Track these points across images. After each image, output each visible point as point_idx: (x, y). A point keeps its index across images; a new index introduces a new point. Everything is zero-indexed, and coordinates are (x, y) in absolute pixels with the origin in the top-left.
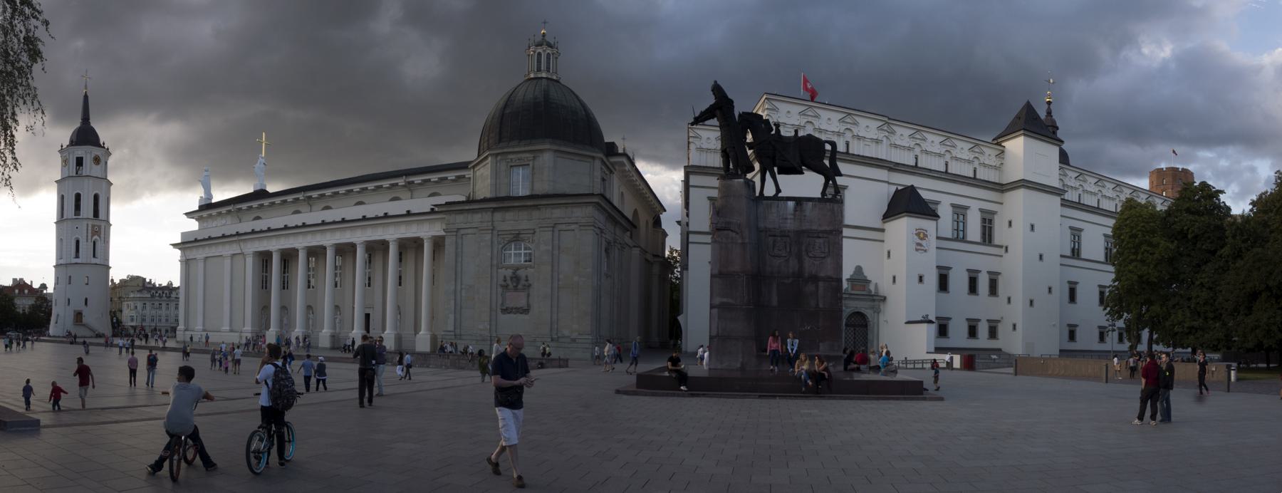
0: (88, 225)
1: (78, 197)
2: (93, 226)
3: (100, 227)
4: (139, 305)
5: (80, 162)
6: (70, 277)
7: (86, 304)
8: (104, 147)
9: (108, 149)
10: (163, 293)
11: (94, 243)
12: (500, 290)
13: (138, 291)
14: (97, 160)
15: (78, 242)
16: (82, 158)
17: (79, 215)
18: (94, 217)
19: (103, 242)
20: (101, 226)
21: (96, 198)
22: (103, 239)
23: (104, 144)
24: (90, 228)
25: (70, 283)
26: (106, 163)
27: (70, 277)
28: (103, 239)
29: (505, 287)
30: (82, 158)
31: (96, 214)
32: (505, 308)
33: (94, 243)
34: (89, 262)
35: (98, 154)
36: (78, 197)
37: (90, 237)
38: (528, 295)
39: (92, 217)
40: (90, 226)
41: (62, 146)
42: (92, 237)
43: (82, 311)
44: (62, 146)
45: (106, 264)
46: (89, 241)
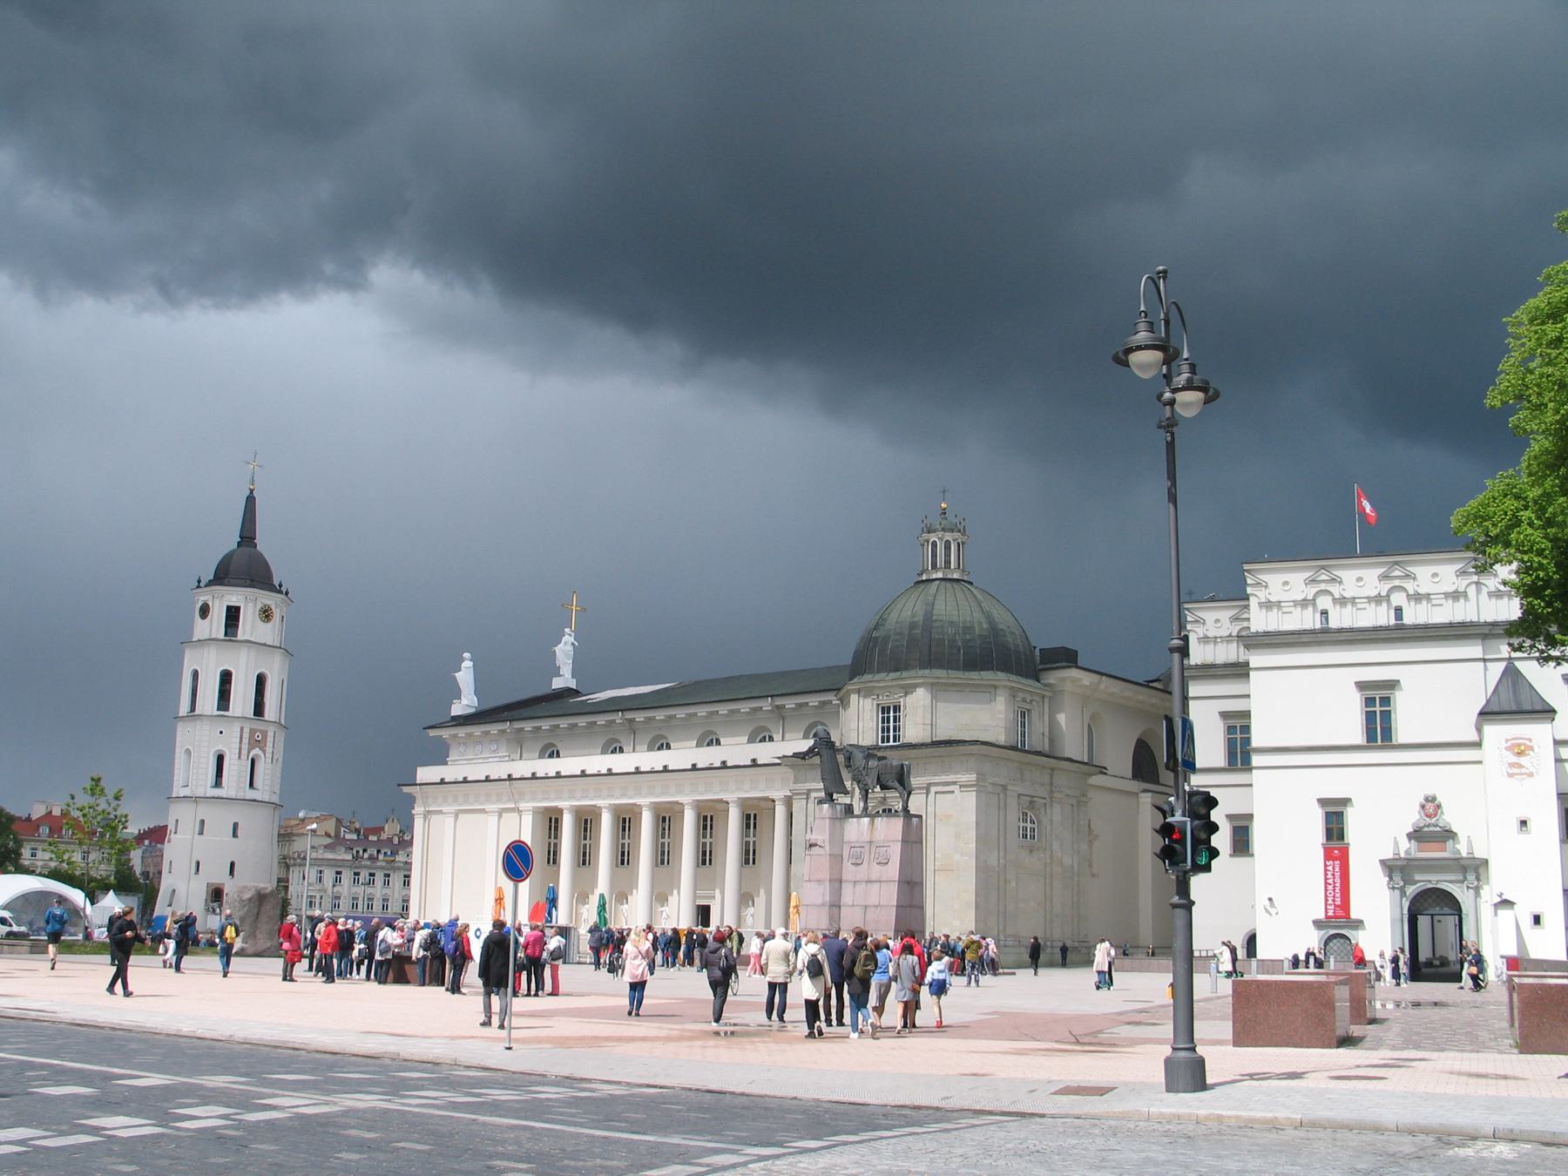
0: (242, 729)
1: (226, 678)
2: (252, 732)
4: (329, 875)
5: (233, 615)
6: (202, 822)
7: (232, 872)
9: (287, 593)
10: (379, 852)
13: (325, 847)
15: (220, 759)
16: (238, 609)
17: (227, 709)
20: (267, 731)
23: (280, 586)
25: (201, 833)
27: (202, 822)
28: (269, 755)
30: (238, 609)
31: (259, 709)
34: (241, 795)
35: (268, 602)
36: (226, 678)
37: (244, 752)
39: (252, 716)
40: (247, 731)
41: (199, 582)
43: (223, 884)
44: (199, 582)
46: (244, 756)
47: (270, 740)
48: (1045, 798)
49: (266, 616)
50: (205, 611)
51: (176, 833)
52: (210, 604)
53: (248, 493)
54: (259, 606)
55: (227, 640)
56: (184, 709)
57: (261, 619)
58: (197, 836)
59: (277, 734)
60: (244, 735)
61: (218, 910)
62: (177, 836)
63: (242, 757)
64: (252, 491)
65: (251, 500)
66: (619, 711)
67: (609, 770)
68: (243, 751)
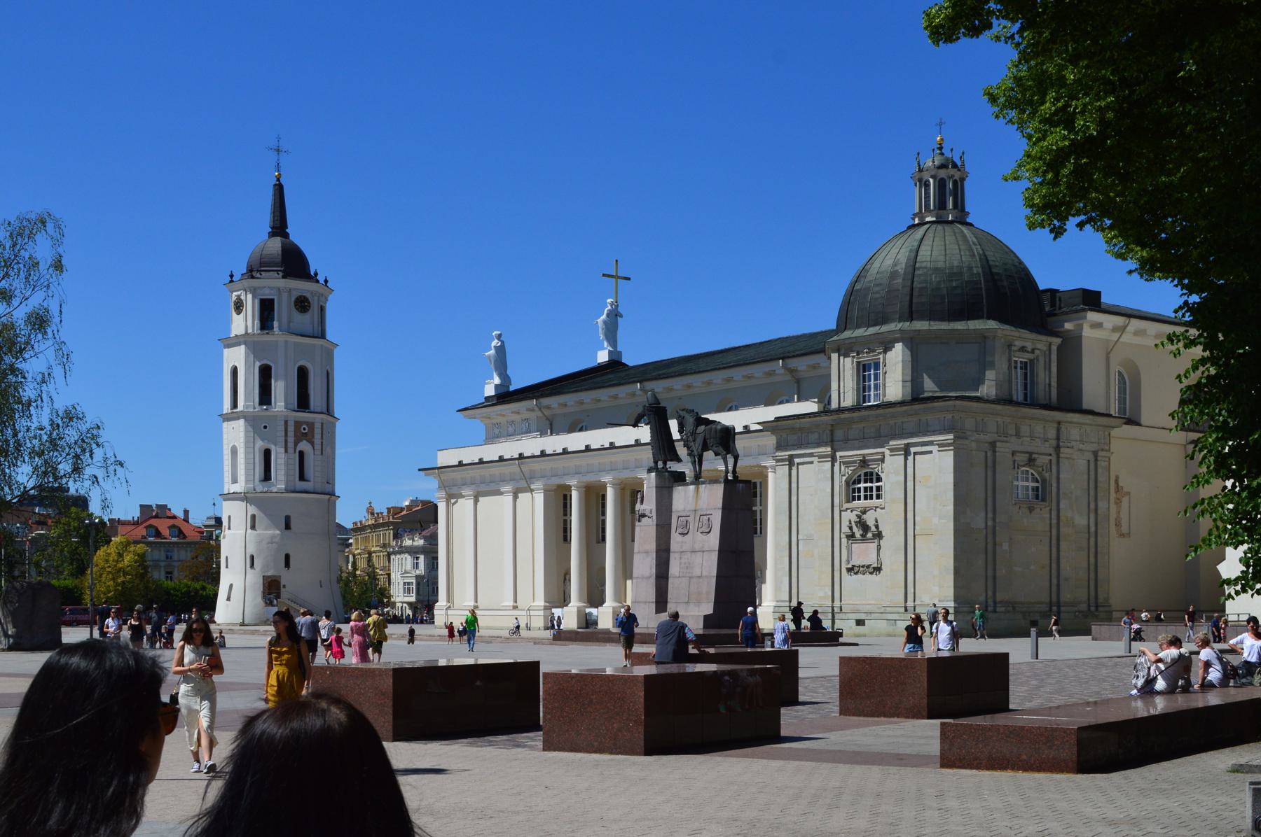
2: (298, 424)
3: (311, 425)
7: (287, 564)
8: (318, 281)
9: (326, 281)
11: (301, 454)
12: (844, 540)
14: (302, 304)
16: (272, 301)
18: (299, 406)
19: (318, 452)
21: (303, 374)
22: (318, 447)
23: (316, 274)
24: (291, 429)
26: (322, 309)
28: (318, 447)
29: (851, 536)
30: (272, 301)
31: (303, 402)
32: (850, 566)
33: (301, 454)
37: (291, 445)
38: (879, 548)
39: (296, 409)
41: (232, 276)
42: (296, 445)
43: (280, 576)
44: (232, 276)
45: (328, 488)
46: (291, 450)
47: (317, 431)
48: (1050, 455)
49: (301, 307)
50: (239, 306)
51: (229, 528)
52: (243, 297)
53: (274, 181)
54: (293, 299)
55: (263, 334)
56: (227, 407)
57: (297, 309)
58: (249, 531)
59: (324, 426)
60: (289, 430)
61: (275, 602)
62: (230, 531)
63: (289, 451)
64: (278, 180)
65: (279, 189)
66: (637, 382)
67: (611, 444)
68: (289, 444)
